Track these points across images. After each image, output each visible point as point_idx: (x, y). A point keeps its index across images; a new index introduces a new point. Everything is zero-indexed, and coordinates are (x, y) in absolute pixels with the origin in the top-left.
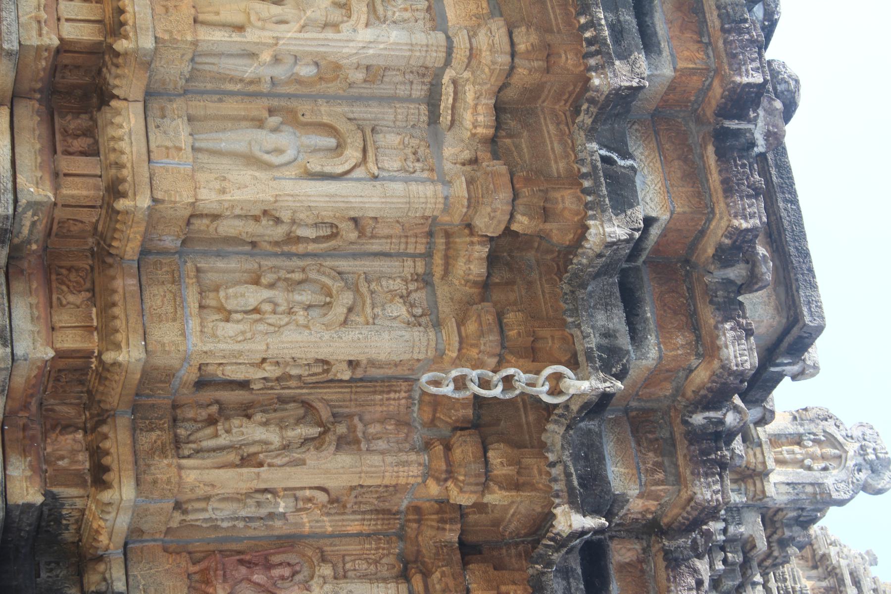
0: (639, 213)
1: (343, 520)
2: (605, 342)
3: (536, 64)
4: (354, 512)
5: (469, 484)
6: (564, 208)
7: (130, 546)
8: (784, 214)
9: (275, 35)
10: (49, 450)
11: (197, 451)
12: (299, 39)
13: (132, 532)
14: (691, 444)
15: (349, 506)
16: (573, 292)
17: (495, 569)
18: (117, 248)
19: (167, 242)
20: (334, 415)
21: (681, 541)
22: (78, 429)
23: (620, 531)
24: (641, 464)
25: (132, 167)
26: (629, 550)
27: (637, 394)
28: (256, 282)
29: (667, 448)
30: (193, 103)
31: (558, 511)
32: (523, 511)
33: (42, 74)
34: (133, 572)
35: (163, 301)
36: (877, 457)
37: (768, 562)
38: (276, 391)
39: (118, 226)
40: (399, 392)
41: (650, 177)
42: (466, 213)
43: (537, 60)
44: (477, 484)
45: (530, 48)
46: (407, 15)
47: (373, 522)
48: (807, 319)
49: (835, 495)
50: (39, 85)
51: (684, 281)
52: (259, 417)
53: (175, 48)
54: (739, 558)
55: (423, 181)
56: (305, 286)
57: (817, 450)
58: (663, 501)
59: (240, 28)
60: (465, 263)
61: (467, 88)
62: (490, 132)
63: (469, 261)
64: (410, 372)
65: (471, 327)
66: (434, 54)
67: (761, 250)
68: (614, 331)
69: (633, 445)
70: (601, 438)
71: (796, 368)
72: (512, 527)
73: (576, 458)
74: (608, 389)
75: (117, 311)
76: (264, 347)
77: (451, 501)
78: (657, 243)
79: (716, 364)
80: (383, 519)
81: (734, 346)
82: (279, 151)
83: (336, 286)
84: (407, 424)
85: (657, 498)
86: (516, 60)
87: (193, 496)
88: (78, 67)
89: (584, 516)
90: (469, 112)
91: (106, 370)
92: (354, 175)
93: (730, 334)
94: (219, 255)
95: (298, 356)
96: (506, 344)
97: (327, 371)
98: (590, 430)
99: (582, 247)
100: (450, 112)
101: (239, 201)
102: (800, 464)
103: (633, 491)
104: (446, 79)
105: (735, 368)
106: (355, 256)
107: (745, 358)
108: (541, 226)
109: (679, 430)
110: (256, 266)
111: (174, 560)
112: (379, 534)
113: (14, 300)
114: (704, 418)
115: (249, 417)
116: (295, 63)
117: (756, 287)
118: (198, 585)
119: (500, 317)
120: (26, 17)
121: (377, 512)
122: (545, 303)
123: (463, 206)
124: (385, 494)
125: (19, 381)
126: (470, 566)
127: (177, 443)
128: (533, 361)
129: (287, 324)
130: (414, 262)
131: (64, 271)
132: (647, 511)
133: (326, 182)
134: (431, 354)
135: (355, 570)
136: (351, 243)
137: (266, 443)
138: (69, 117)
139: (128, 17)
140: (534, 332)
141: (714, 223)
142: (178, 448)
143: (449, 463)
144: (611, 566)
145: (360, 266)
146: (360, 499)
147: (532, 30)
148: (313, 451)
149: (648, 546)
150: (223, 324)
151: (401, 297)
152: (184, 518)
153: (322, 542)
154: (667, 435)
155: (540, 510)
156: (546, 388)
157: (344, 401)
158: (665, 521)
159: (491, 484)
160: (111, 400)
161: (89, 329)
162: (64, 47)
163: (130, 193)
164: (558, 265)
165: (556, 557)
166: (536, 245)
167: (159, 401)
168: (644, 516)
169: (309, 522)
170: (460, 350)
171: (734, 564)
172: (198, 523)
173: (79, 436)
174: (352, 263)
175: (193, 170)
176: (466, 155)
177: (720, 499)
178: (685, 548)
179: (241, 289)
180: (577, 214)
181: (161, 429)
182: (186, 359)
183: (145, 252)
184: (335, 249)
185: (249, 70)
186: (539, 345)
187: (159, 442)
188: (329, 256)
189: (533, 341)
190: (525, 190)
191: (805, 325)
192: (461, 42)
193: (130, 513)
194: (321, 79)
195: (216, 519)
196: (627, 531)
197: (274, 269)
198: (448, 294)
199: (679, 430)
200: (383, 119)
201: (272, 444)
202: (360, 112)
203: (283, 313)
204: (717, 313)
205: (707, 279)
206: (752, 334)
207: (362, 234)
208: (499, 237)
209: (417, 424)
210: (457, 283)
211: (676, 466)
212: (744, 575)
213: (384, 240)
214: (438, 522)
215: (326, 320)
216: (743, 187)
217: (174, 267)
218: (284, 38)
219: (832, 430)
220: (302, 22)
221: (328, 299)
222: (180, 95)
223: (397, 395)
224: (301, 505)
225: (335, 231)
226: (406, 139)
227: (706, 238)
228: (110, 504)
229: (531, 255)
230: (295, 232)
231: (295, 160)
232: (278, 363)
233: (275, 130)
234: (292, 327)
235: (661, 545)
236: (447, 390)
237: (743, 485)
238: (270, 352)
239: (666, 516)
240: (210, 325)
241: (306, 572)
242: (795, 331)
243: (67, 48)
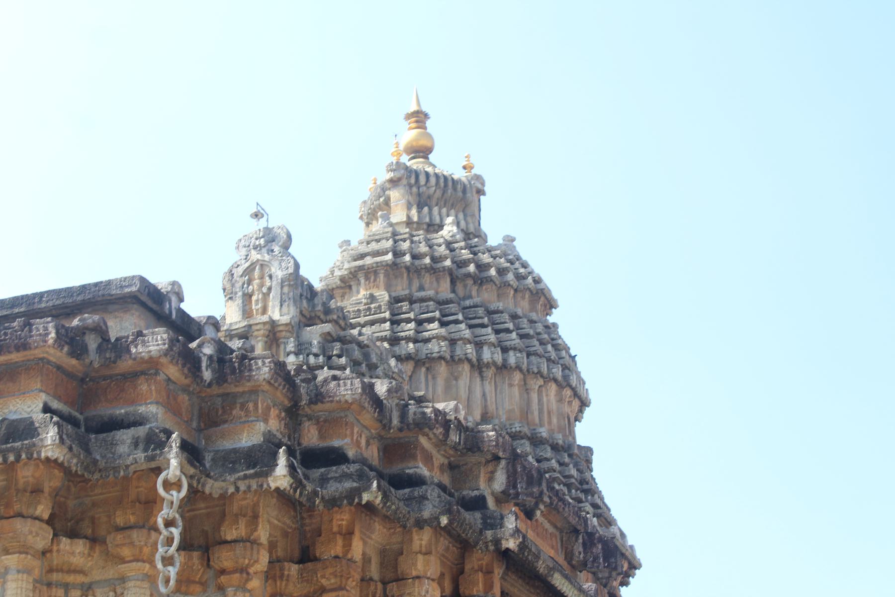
0: (39, 417)
2: (141, 446)
5: (252, 555)
6: (33, 476)
8: (51, 304)
14: (226, 381)
16: (100, 471)
17: (320, 535)
21: (303, 391)
23: (294, 438)
24: (241, 420)
26: (309, 431)
27: (187, 421)
29: (230, 400)
31: (273, 485)
32: (275, 513)
36: (263, 237)
37: (342, 323)
41: (11, 407)
42: (32, 555)
44: (252, 549)
48: (134, 289)
49: (291, 270)
51: (98, 383)
54: (337, 346)
57: (256, 282)
58: (272, 404)
60: (75, 557)
63: (73, 553)
65: (126, 552)
67: (76, 322)
68: (133, 439)
69: (226, 426)
70: (218, 451)
71: (174, 299)
72: (288, 522)
73: (233, 471)
74: (178, 444)
78: (65, 404)
79: (164, 360)
81: (150, 346)
85: (268, 409)
89: (277, 465)
93: (140, 349)
96: (141, 524)
98: (213, 459)
99: (62, 463)
102: (266, 296)
103: (261, 427)
105: (167, 346)
107: (159, 337)
108: (46, 495)
109: (215, 390)
114: (207, 370)
117: (104, 327)
119: (119, 529)
122: (110, 492)
123: (26, 558)
126: (318, 555)
128: (155, 503)
132: (278, 416)
134: (146, 585)
140: (132, 502)
141: (51, 359)
143: (235, 571)
144: (321, 445)
149: (306, 416)
154: (220, 399)
155: (275, 500)
156: (174, 493)
158: (287, 403)
159: (252, 538)
164: (80, 482)
165: (309, 488)
168: (283, 419)
170: (144, 561)
171: (342, 349)
177: (269, 360)
178: (308, 388)
180: (37, 466)
189: (140, 503)
190: (15, 507)
191: (138, 291)
196: (294, 433)
199: (215, 390)
204: (123, 358)
205: (96, 365)
206: (141, 332)
208: (54, 529)
210: (90, 564)
211: (244, 393)
212: (350, 342)
214: (282, 580)
216: (23, 335)
219: (240, 270)
227: (64, 365)
229: (71, 503)
235: (306, 407)
236: (172, 571)
237: (281, 340)
239: (283, 402)
242: (144, 298)
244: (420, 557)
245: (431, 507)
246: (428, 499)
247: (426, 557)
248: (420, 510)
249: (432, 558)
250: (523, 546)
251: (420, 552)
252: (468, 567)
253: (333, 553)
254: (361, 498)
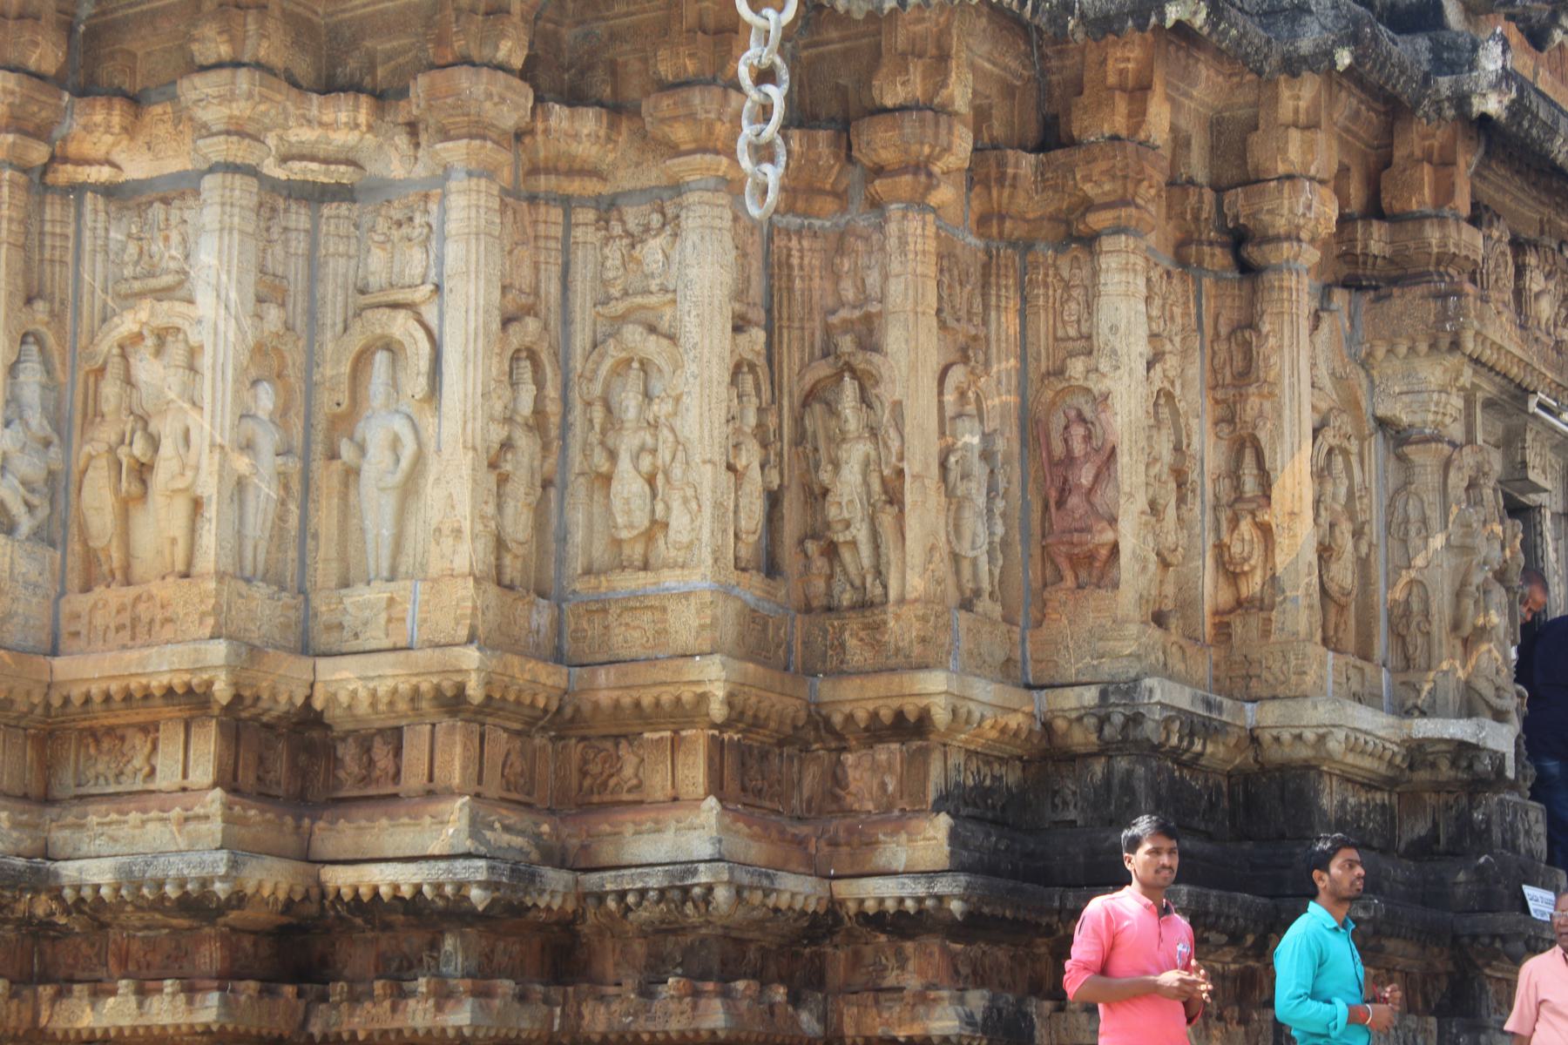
1: (998, 340)
3: (252, 27)
4: (985, 323)
5: (936, 135)
7: (1031, 680)
9: (207, 449)
10: (870, 806)
11: (878, 573)
12: (213, 411)
13: (1008, 676)
15: (973, 332)
17: (1081, 93)
18: (548, 699)
19: (542, 622)
20: (825, 355)
22: (839, 762)
25: (417, 675)
28: (607, 479)
30: (320, 580)
33: (269, 816)
34: (1071, 674)
35: (635, 628)
38: (786, 448)
39: (512, 698)
40: (789, 250)
42: (494, 142)
43: (245, 25)
44: (937, 124)
45: (225, 37)
46: (175, 237)
47: (1003, 292)
50: (289, 820)
52: (825, 476)
53: (229, 609)
55: (444, 211)
56: (614, 401)
59: (197, 505)
60: (580, 143)
61: (293, 139)
62: (364, 100)
63: (576, 136)
64: (757, 233)
65: (681, 133)
66: (237, 193)
72: (1014, 65)
75: (647, 700)
76: (709, 467)
77: (967, 165)
80: (998, 276)
82: (395, 443)
83: (613, 352)
84: (842, 236)
86: (246, 59)
87: (951, 581)
88: (261, 760)
90: (332, 135)
91: (737, 716)
92: (433, 322)
94: (563, 539)
95: (724, 413)
96: (709, 76)
97: (752, 367)
100: (333, 167)
101: (473, 507)
104: (280, 173)
106: (567, 321)
108: (516, 19)
110: (581, 480)
111: (1055, 610)
112: (1022, 282)
113: (627, 858)
115: (825, 492)
116: (254, 417)
118: (1095, 573)
120: (179, 840)
121: (985, 285)
122: (644, 11)
123: (483, 147)
124: (956, 272)
125: (756, 851)
126: (1076, 133)
127: (864, 605)
128: (737, 32)
129: (672, 430)
130: (577, 225)
131: (587, 782)
133: (445, 369)
134: (723, 199)
135: (1079, 321)
136: (546, 327)
137: (866, 464)
138: (342, 774)
139: (178, 681)
140: (688, 31)
142: (872, 604)
143: (903, 170)
145: (583, 312)
146: (963, 314)
147: (195, 32)
148: (881, 390)
150: (671, 533)
151: (633, 246)
152: (986, 595)
153: (1033, 375)
155: (984, 20)
156: (770, 13)
157: (803, 339)
159: (937, 100)
160: (791, 710)
161: (675, 744)
162: (228, 780)
163: (458, 678)
166: (550, 26)
167: (798, 634)
169: (999, 395)
170: (717, 152)
172: (997, 572)
173: (849, 758)
174: (578, 326)
175: (425, 580)
176: (402, 140)
179: (617, 505)
181: (842, 629)
182: (726, 591)
183: (558, 657)
184: (556, 354)
185: (265, 490)
186: (710, 22)
187: (862, 634)
188: (566, 364)
189: (705, 32)
190: (456, 45)
192: (219, 149)
193: (971, 679)
194: (279, 376)
195: (991, 543)
197: (586, 449)
198: (631, 170)
200: (345, 275)
201: (868, 456)
202: (334, 312)
203: (656, 437)
207: (531, 310)
208: (536, 88)
209: (843, 221)
210: (611, 156)
213: (543, 275)
214: (1003, 186)
215: (667, 369)
217: (581, 610)
218: (212, 436)
220: (187, 406)
221: (635, 365)
222: (307, 600)
223: (795, 253)
224: (971, 408)
225: (524, 354)
226: (377, 238)
228: (954, 712)
229: (569, 34)
230: (526, 419)
231: (409, 417)
232: (737, 446)
233: (362, 449)
234: (677, 423)
236: (772, 174)
238: (717, 458)
240: (673, 553)
241: (1081, 401)
243: (229, 777)
244: (1295, 135)
245: (1317, 28)
246: (1310, 12)
247: (1308, 133)
248: (1294, 36)
249: (1321, 137)
250: (1517, 109)
251: (1296, 125)
252: (1399, 153)
253: (1107, 130)
254: (1162, 16)
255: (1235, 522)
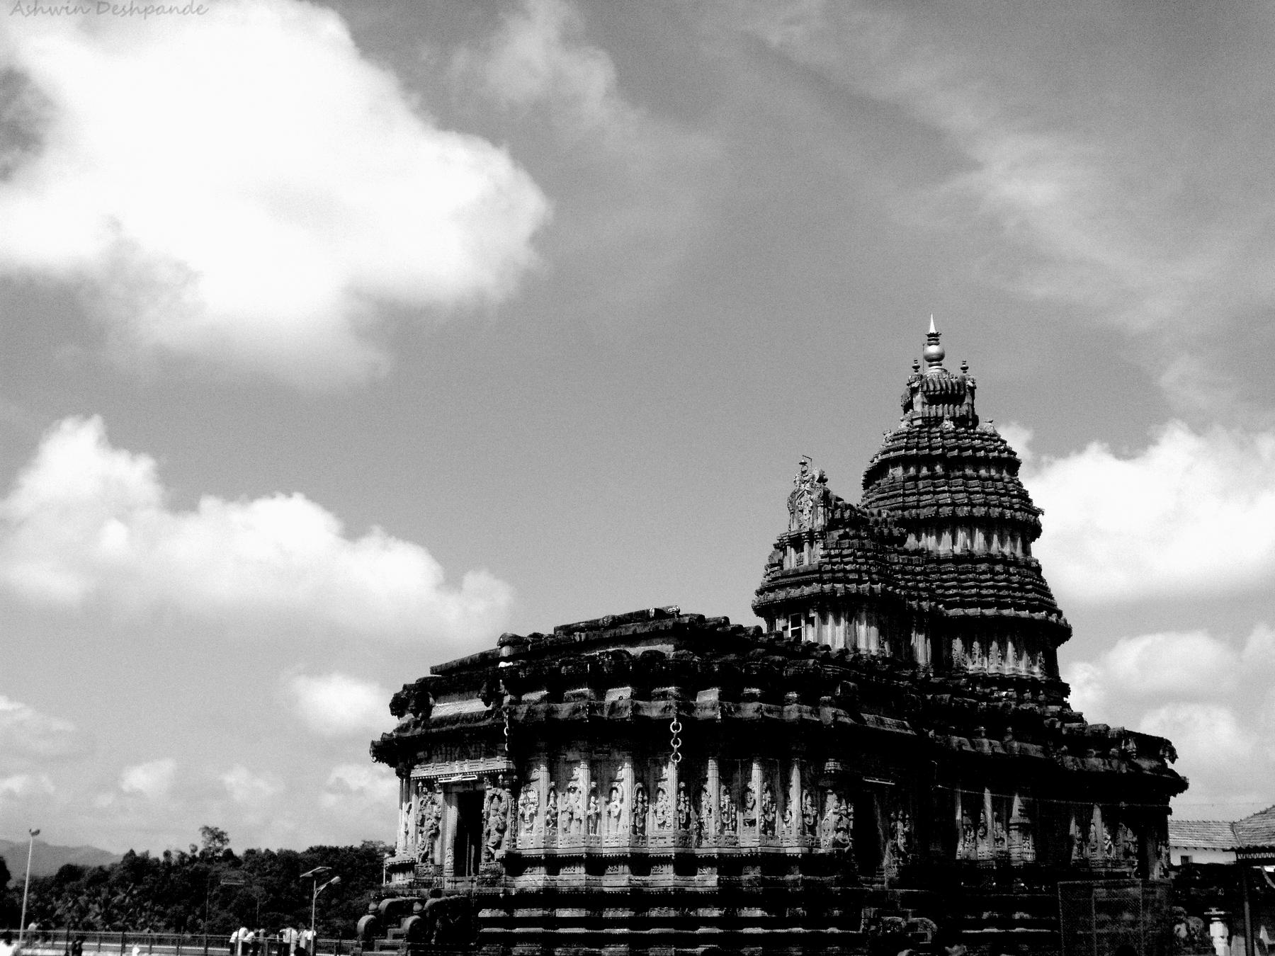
255: (785, 811)
